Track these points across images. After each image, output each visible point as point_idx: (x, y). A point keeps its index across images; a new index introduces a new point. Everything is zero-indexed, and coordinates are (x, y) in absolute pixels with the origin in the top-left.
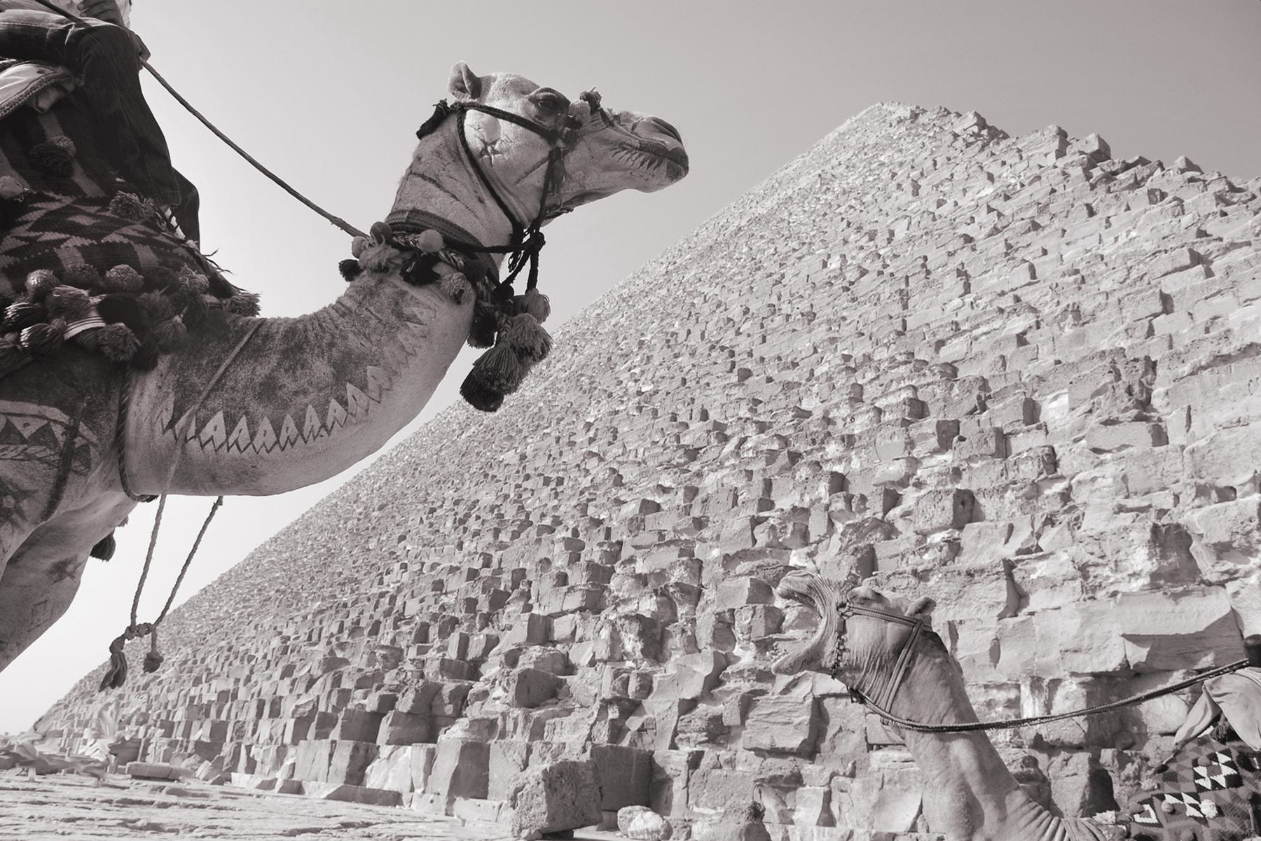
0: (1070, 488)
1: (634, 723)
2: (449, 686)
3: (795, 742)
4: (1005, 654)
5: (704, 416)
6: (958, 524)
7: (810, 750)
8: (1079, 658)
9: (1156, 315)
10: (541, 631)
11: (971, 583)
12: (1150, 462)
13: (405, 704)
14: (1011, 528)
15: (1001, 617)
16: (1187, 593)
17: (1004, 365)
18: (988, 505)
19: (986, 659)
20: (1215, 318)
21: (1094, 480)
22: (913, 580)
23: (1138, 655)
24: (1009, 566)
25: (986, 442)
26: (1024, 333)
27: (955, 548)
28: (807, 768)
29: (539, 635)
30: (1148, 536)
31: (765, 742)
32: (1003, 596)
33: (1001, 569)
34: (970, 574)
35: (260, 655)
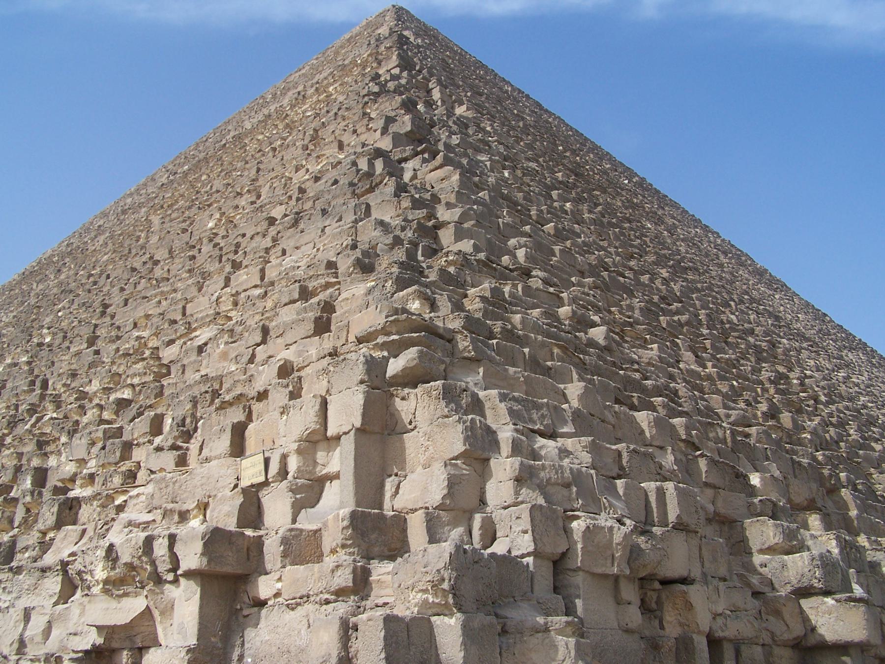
0: (125, 501)
4: (55, 633)
6: (59, 525)
8: (77, 638)
9: (258, 345)
11: (43, 577)
12: (164, 485)
14: (84, 531)
15: (56, 604)
16: (126, 595)
17: (183, 372)
18: (85, 513)
19: (39, 638)
20: (270, 357)
21: (138, 495)
22: (11, 575)
24: (64, 564)
25: (114, 453)
26: (206, 344)
27: (45, 546)
30: (104, 554)
32: (58, 588)
33: (59, 567)
34: (44, 570)
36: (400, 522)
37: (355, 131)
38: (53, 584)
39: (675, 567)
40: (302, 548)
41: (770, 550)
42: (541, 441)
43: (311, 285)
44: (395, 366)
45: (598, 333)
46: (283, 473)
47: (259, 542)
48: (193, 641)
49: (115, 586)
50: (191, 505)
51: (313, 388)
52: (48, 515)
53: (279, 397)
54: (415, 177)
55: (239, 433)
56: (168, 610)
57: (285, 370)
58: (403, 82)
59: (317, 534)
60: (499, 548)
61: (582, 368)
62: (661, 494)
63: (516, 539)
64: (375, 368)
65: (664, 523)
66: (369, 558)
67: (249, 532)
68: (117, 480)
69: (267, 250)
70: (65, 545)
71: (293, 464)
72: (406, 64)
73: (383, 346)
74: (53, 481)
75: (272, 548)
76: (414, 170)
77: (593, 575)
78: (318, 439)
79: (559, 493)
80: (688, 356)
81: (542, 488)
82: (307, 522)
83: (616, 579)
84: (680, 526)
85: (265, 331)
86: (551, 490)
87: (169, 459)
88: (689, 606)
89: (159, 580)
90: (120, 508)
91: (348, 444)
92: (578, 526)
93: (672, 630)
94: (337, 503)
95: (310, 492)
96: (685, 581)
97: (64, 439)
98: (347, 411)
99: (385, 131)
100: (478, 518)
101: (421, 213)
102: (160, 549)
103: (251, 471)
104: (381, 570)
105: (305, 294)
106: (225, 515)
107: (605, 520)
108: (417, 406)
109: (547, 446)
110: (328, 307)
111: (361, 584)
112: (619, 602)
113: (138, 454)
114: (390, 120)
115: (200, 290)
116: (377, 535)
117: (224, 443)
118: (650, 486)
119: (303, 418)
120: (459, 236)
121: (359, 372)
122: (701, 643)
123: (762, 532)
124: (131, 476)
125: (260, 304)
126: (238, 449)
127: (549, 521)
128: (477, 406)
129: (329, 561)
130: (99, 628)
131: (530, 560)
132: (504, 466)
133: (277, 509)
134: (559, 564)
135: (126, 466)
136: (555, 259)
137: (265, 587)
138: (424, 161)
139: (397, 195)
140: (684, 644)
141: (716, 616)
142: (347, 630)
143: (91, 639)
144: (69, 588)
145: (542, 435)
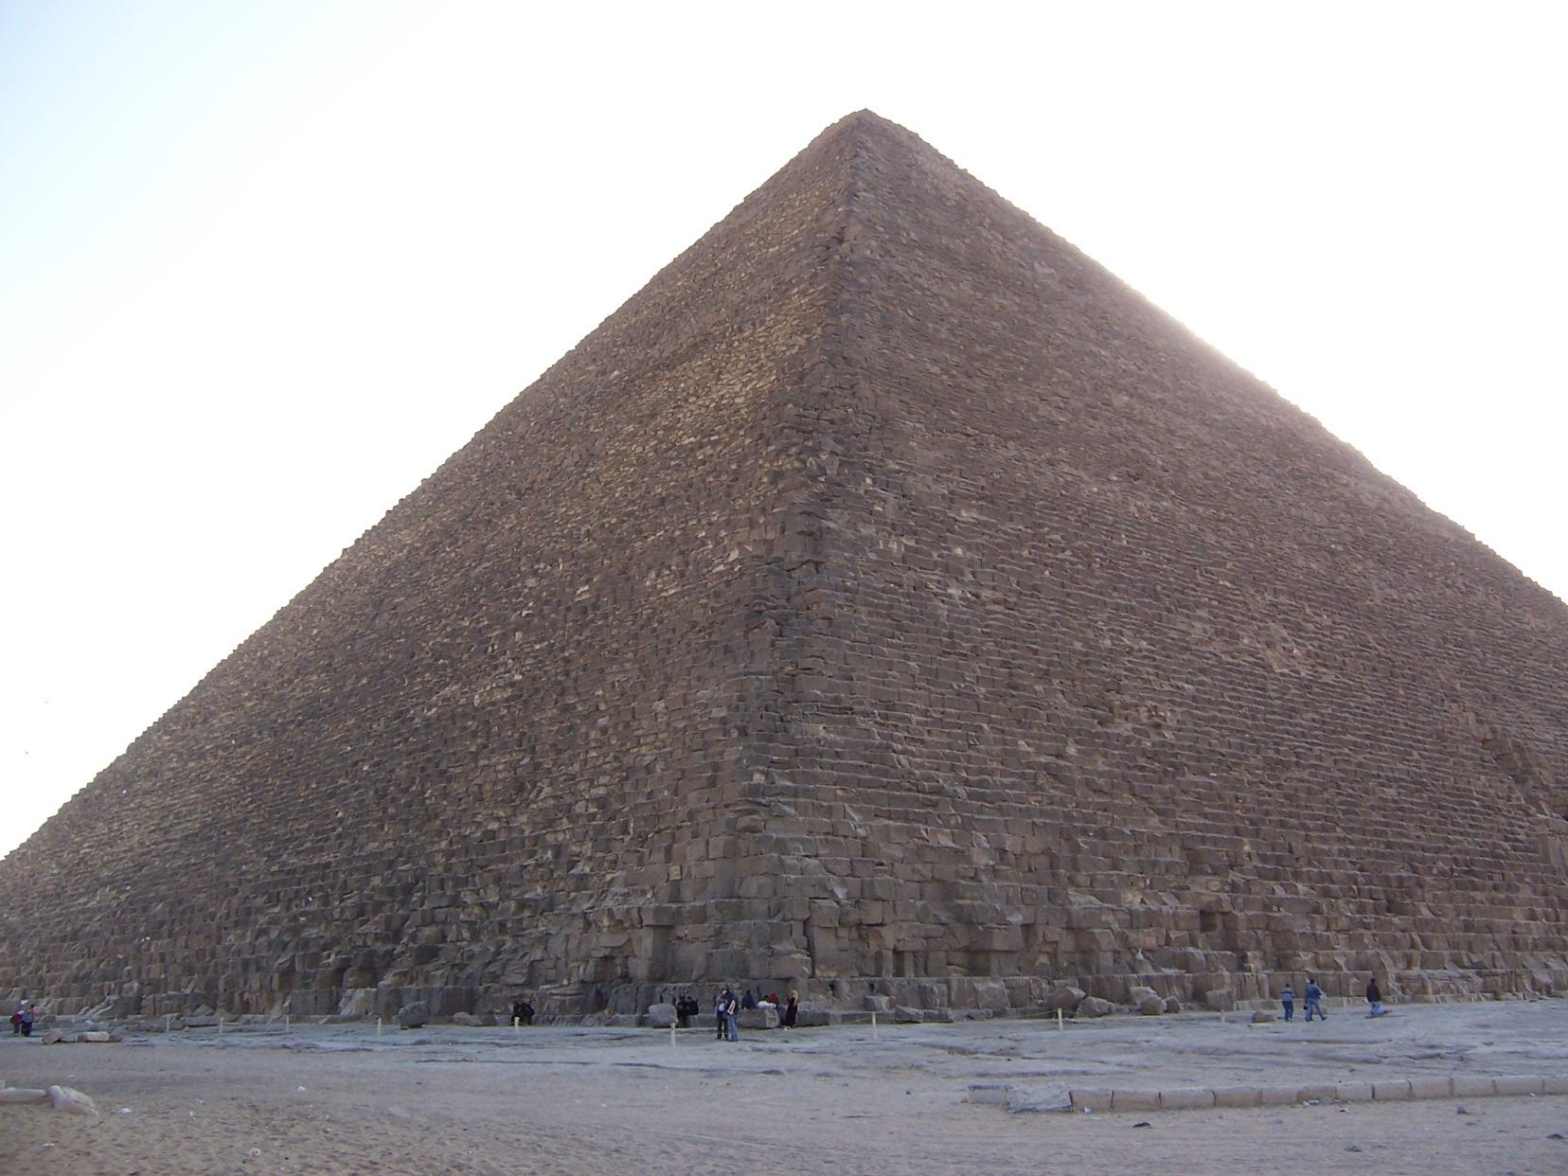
1: (463, 976)
2: (381, 948)
23: (607, 952)
38: (580, 923)
39: (875, 918)
53: (688, 833)
55: (669, 849)
67: (674, 906)
87: (634, 858)
93: (874, 948)
96: (881, 925)
113: (618, 849)
117: (659, 857)
135: (611, 857)
140: (878, 957)
144: (588, 924)
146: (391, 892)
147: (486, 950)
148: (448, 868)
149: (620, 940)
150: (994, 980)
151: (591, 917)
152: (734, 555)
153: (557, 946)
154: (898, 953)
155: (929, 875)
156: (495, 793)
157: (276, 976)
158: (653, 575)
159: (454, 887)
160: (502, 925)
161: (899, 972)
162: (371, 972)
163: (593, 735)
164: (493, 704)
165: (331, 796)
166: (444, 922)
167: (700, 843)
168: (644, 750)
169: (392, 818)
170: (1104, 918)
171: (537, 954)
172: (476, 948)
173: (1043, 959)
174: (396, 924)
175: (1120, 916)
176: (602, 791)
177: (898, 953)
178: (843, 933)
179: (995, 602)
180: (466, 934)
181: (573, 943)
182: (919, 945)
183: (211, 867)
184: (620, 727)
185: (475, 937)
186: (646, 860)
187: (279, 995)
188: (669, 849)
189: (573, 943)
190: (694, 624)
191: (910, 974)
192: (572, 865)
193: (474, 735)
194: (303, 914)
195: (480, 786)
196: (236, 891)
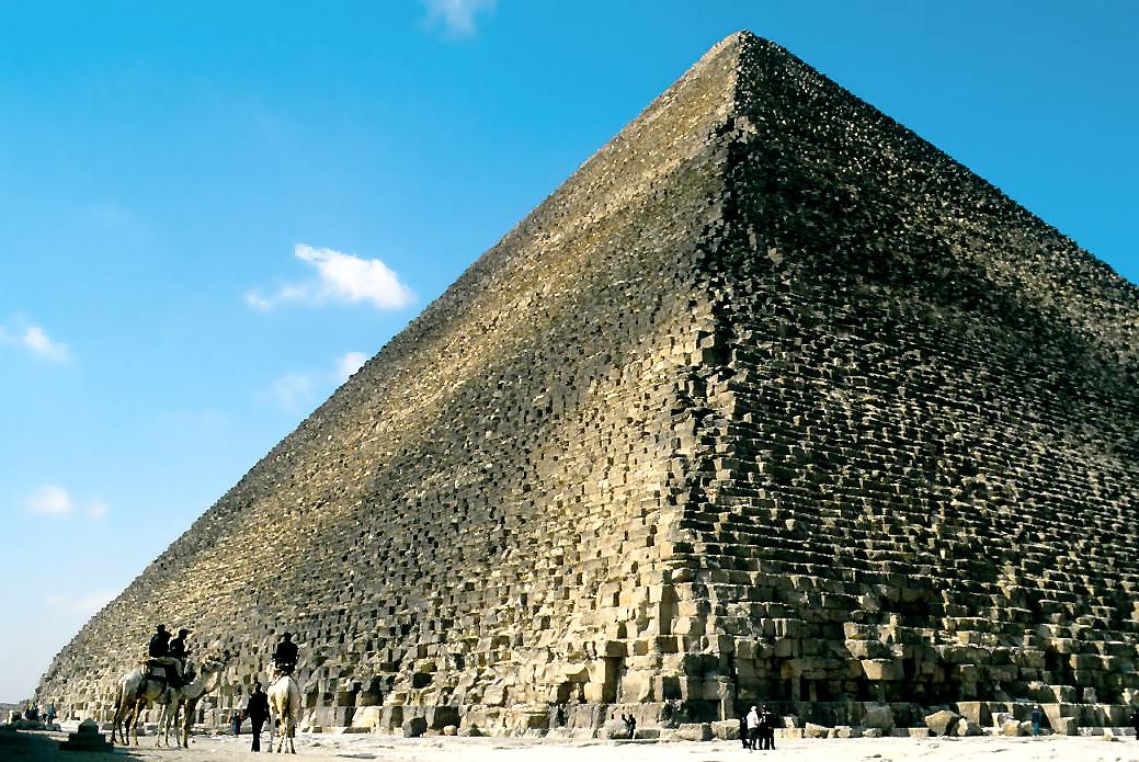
1: (451, 697)
2: (385, 675)
3: (498, 700)
5: (503, 521)
6: (542, 629)
7: (503, 704)
10: (422, 653)
13: (366, 686)
18: (552, 622)
27: (538, 638)
28: (502, 710)
29: (423, 653)
31: (489, 702)
35: (262, 648)
36: (675, 639)
37: (682, 330)
38: (545, 655)
40: (641, 649)
41: (853, 638)
42: (730, 605)
43: (647, 508)
44: (676, 574)
45: (790, 523)
46: (634, 617)
47: (625, 644)
48: (604, 681)
49: (571, 659)
50: (599, 626)
51: (645, 581)
52: (537, 624)
53: (632, 582)
54: (712, 394)
55: (616, 596)
56: (593, 669)
57: (635, 567)
58: (726, 234)
59: (646, 643)
60: (707, 652)
61: (764, 557)
62: (780, 623)
63: (713, 648)
64: (667, 575)
65: (781, 635)
66: (663, 653)
67: (622, 641)
68: (566, 609)
69: (627, 455)
70: (547, 638)
71: (638, 613)
72: (729, 214)
73: (671, 565)
74: (530, 604)
75: (630, 648)
76: (714, 387)
77: (743, 659)
78: (646, 604)
79: (731, 628)
80: (868, 508)
81: (725, 628)
82: (643, 637)
83: (754, 660)
84: (787, 637)
85: (626, 534)
86: (729, 628)
87: (588, 603)
88: (791, 669)
89: (590, 659)
90: (569, 623)
91: (657, 607)
92: (737, 642)
94: (654, 627)
95: (643, 625)
96: (791, 657)
97: (531, 575)
98: (657, 595)
99: (698, 346)
100: (702, 637)
101: (706, 447)
102: (589, 647)
103: (622, 614)
104: (666, 658)
105: (645, 513)
106: (612, 634)
107: (749, 639)
108: (684, 591)
109: (731, 607)
110: (654, 530)
111: (659, 663)
112: (755, 668)
113: (573, 595)
114: (703, 334)
115: (591, 471)
116: (666, 644)
118: (776, 620)
119: (640, 595)
120: (724, 466)
121: (661, 578)
122: (796, 682)
123: (850, 629)
124: (571, 607)
125: (624, 508)
126: (616, 603)
127: (725, 641)
128: (706, 592)
129: (648, 655)
130: (567, 675)
131: (718, 655)
132: (712, 619)
133: (632, 629)
134: (730, 655)
135: (569, 602)
136: (788, 456)
137: (628, 662)
138: (721, 379)
139: (695, 432)
140: (789, 683)
141: (805, 671)
142: (652, 680)
143: (564, 679)
144: (551, 657)
145: (731, 602)
146: (392, 631)
147: (469, 676)
148: (437, 612)
149: (577, 668)
150: (881, 705)
151: (554, 651)
152: (660, 366)
153: (525, 674)
154: (805, 682)
155: (827, 618)
156: (473, 554)
157: (304, 697)
158: (594, 383)
159: (443, 628)
160: (482, 657)
161: (805, 697)
162: (376, 697)
163: (550, 508)
164: (470, 486)
165: (345, 559)
166: (436, 655)
167: (642, 591)
168: (592, 518)
169: (392, 574)
170: (969, 655)
171: (510, 680)
172: (462, 675)
173: (920, 688)
174: (395, 657)
175: (982, 654)
176: (560, 552)
177: (805, 682)
178: (759, 664)
179: (869, 402)
180: (453, 664)
181: (539, 672)
182: (821, 675)
183: (254, 613)
184: (573, 501)
185: (460, 665)
186: (597, 603)
187: (307, 711)
188: (616, 596)
189: (539, 672)
190: (630, 420)
191: (814, 698)
192: (536, 609)
193: (456, 510)
194: (324, 649)
195: (460, 549)
196: (273, 631)
